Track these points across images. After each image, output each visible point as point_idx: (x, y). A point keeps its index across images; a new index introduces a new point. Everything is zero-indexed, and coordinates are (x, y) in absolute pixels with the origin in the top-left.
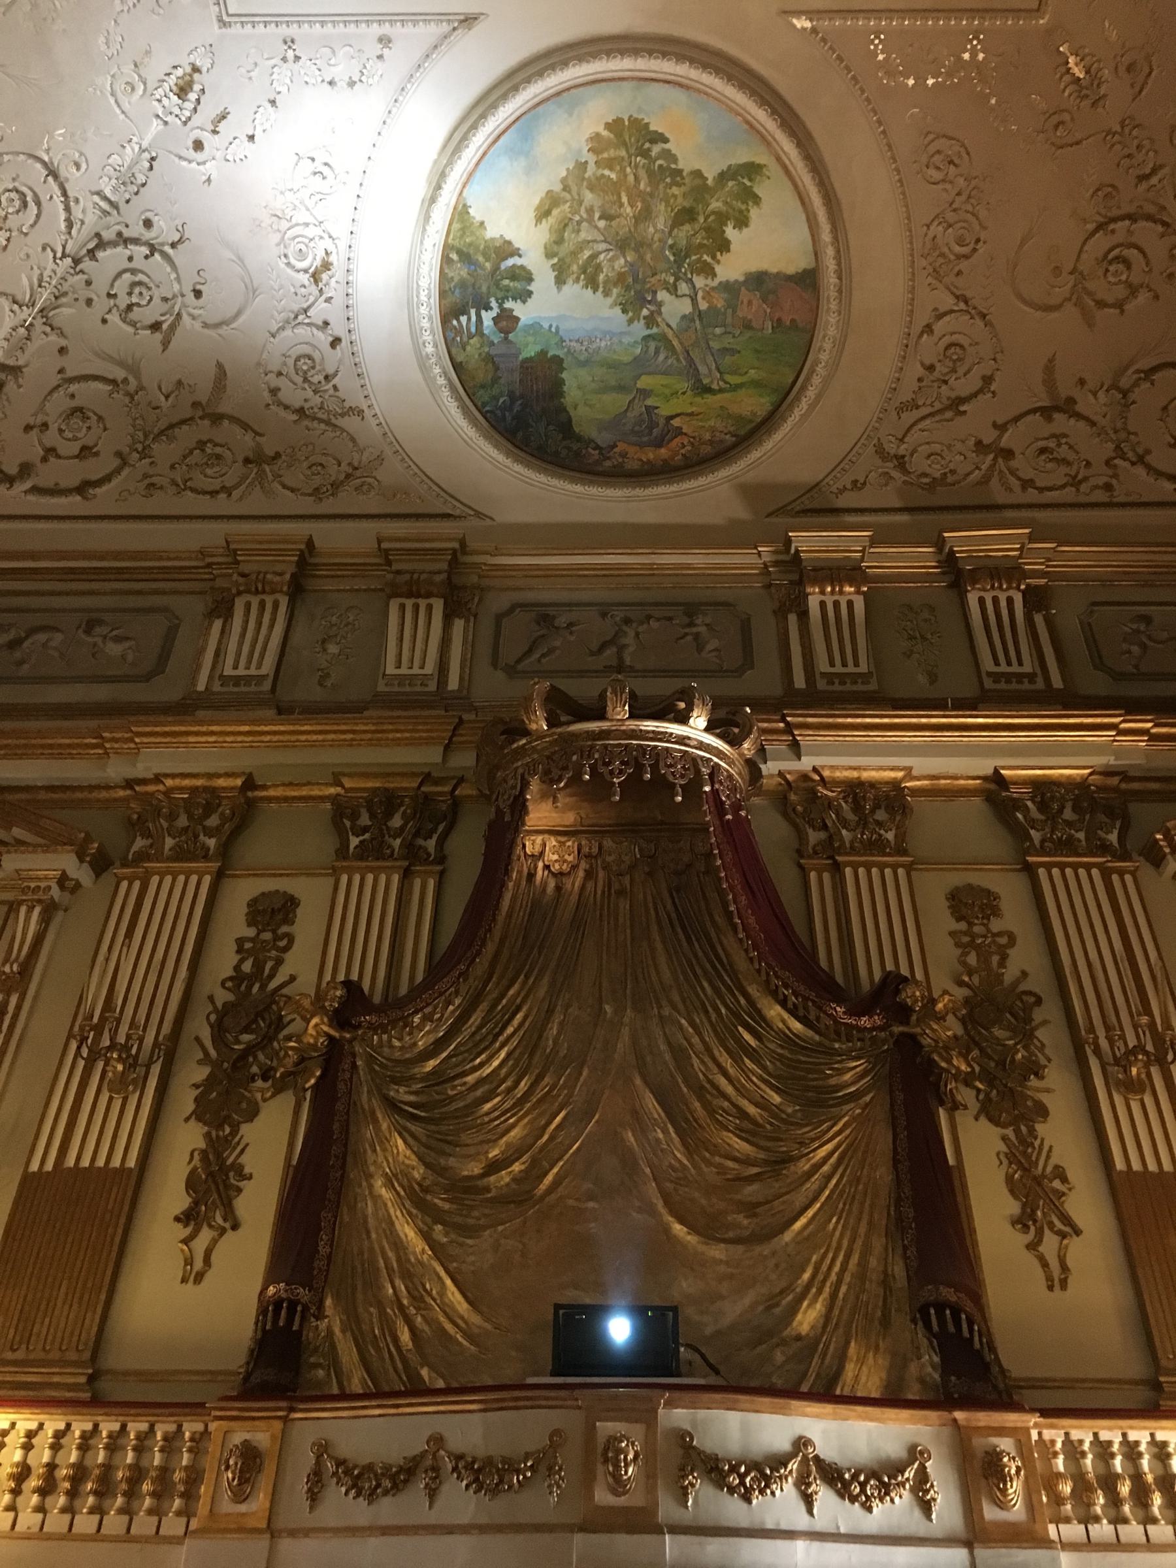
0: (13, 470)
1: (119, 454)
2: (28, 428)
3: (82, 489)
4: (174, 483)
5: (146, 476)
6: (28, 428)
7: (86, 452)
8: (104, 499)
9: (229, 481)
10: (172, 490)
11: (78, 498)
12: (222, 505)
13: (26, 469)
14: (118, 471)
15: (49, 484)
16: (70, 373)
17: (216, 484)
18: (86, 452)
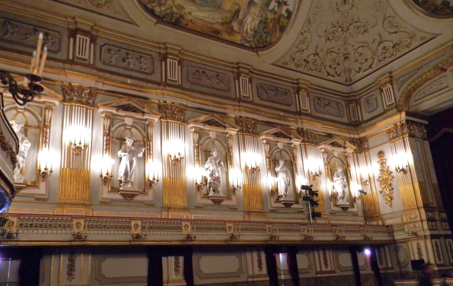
0: (358, 70)
1: (372, 58)
2: (355, 61)
3: (370, 67)
4: (383, 58)
5: (378, 59)
6: (355, 61)
7: (366, 60)
8: (374, 67)
9: (392, 52)
10: (384, 59)
11: (370, 69)
12: (393, 58)
13: (360, 69)
14: (373, 61)
15: (365, 69)
16: (355, 48)
17: (389, 55)
18: (366, 60)
